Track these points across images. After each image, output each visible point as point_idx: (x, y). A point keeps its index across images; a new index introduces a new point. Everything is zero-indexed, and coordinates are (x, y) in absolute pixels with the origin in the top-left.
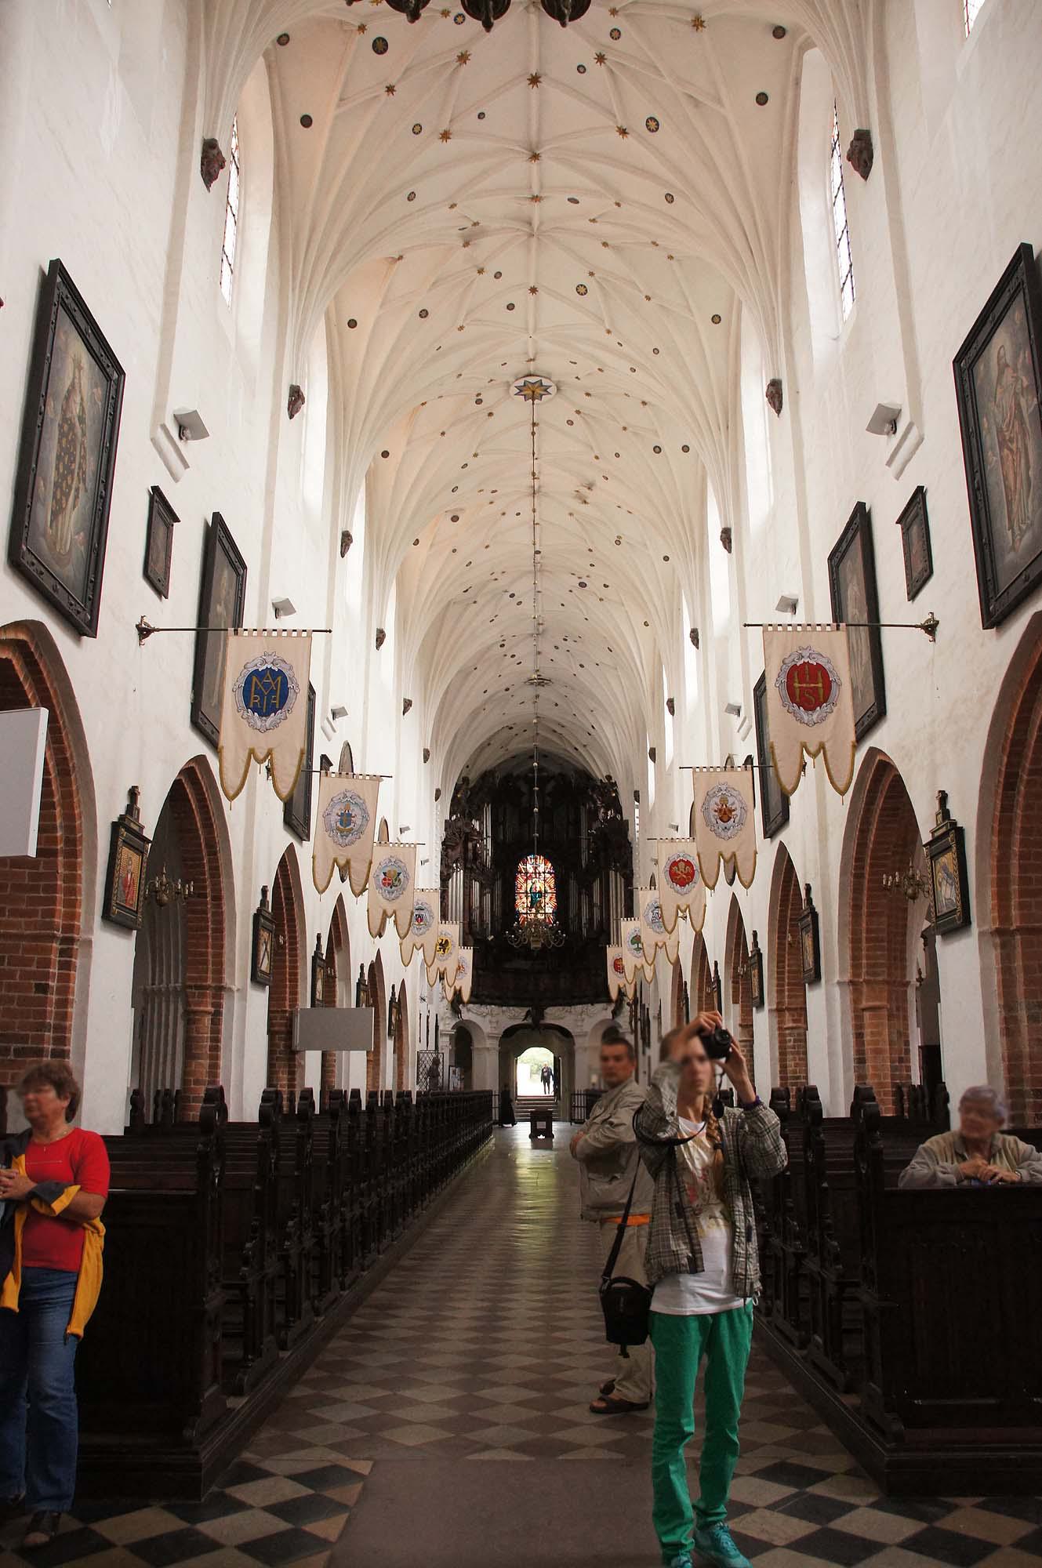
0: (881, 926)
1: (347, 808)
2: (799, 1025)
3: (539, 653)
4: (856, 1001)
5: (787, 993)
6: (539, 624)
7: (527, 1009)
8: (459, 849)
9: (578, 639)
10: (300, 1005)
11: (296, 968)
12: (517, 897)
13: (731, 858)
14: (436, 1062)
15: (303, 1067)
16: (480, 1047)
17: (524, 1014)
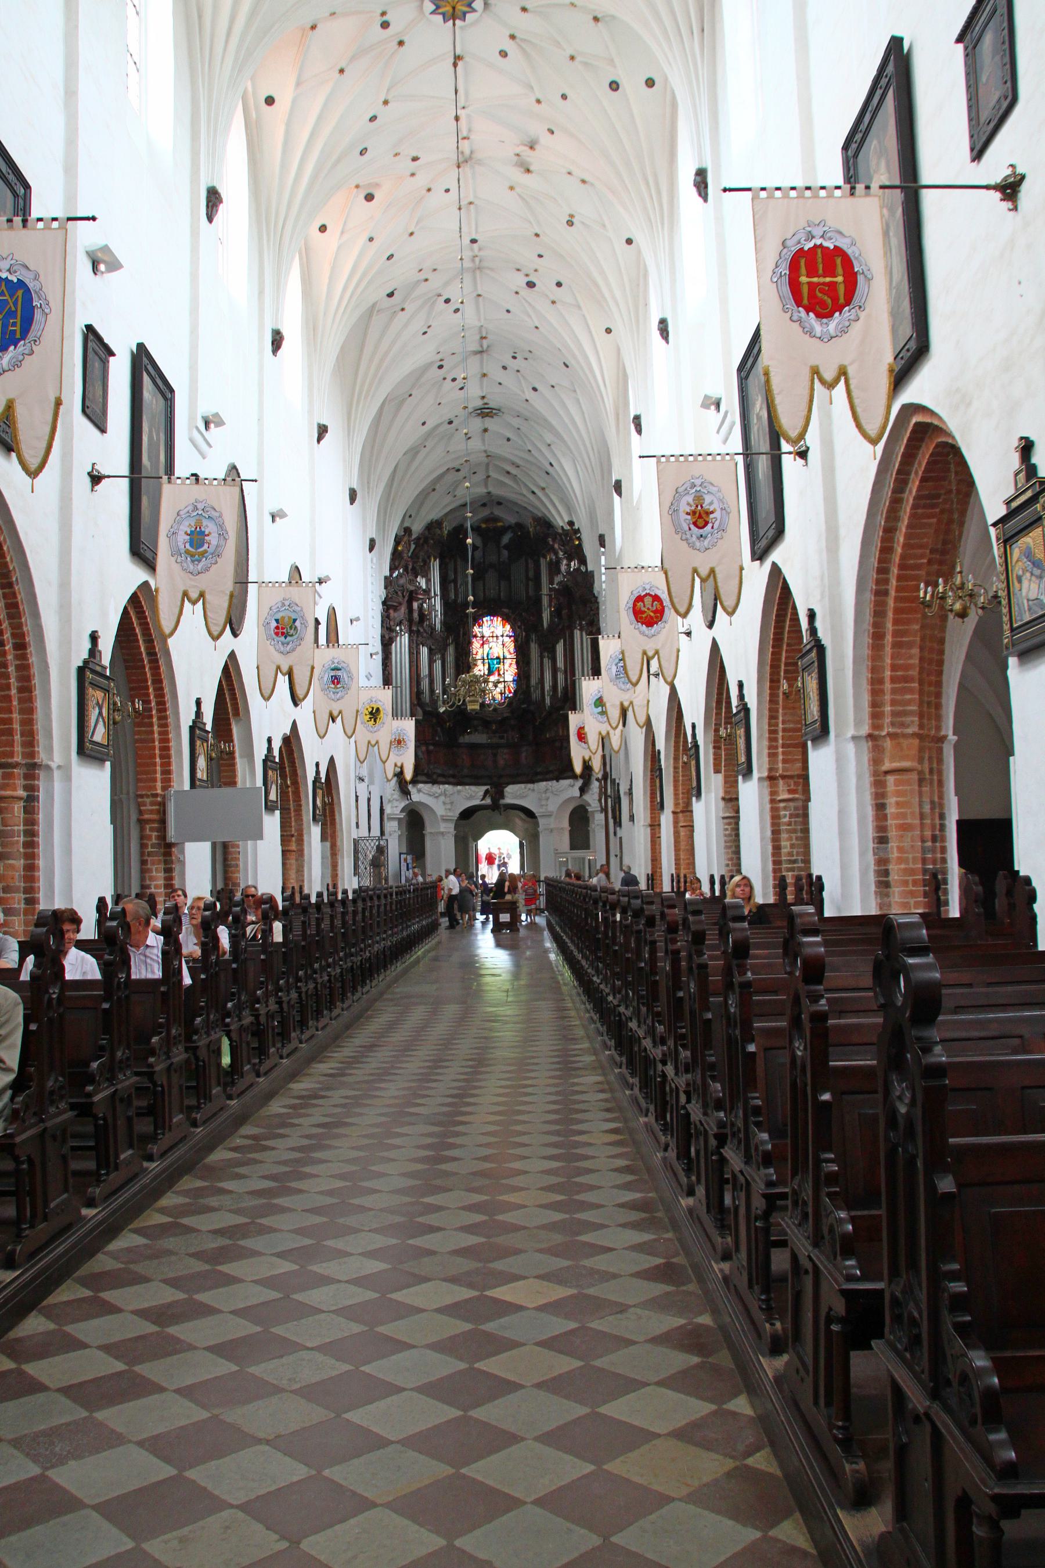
0: (912, 661)
1: (199, 524)
2: (797, 796)
3: (484, 375)
4: (876, 761)
5: (781, 757)
6: (482, 338)
7: (486, 788)
8: (403, 609)
9: (527, 355)
10: (175, 786)
11: (168, 740)
13: (709, 576)
14: (381, 850)
15: (182, 863)
16: (433, 831)
17: (482, 793)
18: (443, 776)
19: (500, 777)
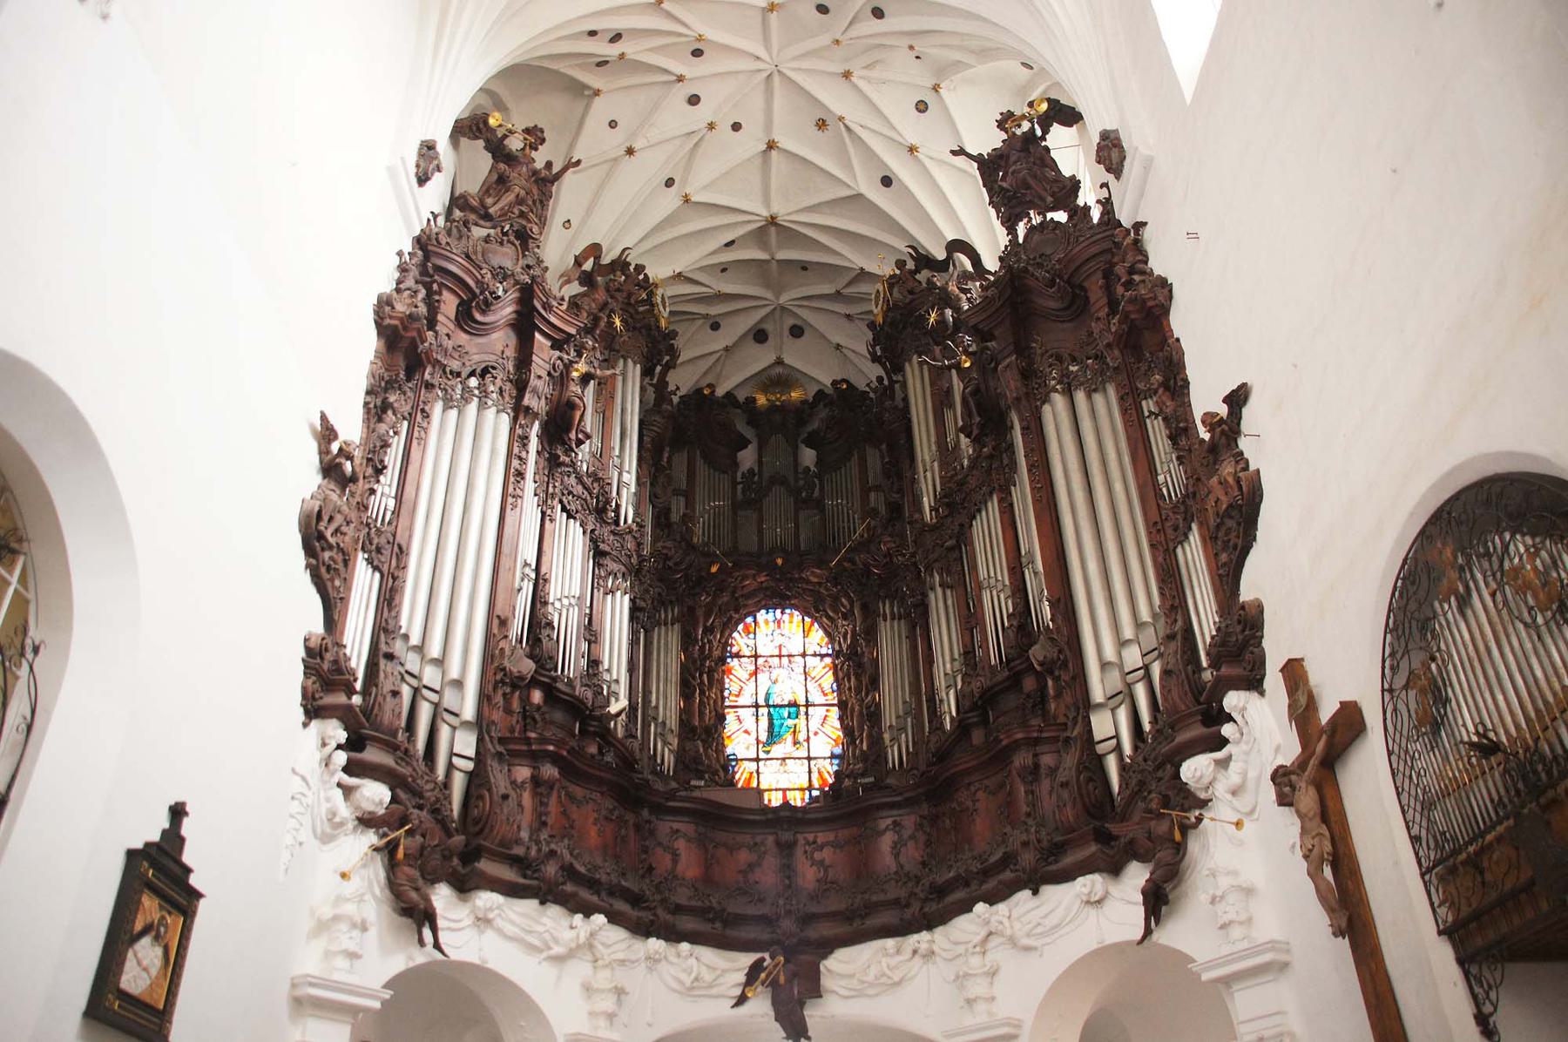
12: (730, 717)
17: (741, 977)
18: (592, 884)
19: (808, 919)
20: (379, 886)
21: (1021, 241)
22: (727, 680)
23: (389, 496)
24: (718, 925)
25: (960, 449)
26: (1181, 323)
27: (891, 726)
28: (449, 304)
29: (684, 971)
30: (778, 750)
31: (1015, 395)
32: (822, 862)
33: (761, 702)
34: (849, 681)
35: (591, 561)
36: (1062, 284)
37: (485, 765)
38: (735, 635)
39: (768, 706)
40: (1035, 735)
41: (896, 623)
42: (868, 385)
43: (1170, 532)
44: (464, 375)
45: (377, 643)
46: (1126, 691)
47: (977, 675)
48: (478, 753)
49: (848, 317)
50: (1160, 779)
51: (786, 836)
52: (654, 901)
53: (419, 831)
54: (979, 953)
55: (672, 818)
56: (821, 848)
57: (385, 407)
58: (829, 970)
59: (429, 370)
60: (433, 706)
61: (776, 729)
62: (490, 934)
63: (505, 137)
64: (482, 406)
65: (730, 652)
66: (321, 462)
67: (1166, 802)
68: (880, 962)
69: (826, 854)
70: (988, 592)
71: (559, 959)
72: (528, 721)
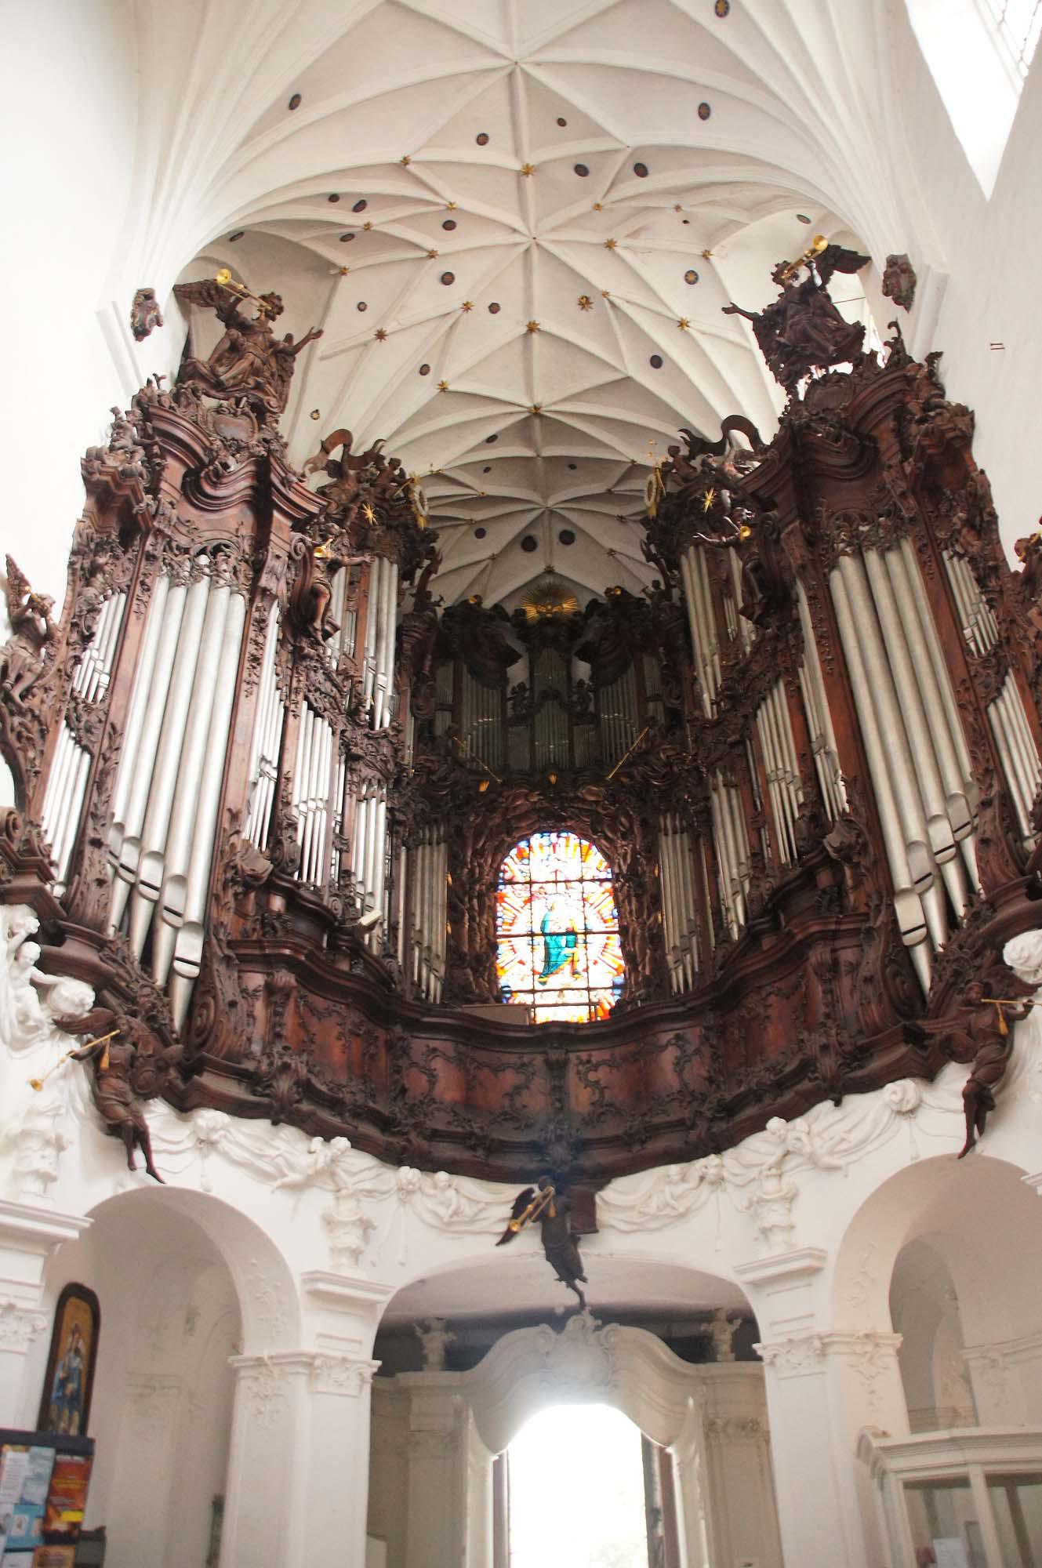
12: (504, 948)
17: (507, 1211)
18: (334, 1104)
19: (582, 1146)
20: (83, 1100)
21: (801, 397)
22: (499, 908)
23: (101, 673)
24: (480, 1153)
25: (742, 636)
26: (983, 454)
27: (675, 947)
28: (174, 472)
29: (442, 1204)
30: (554, 981)
31: (799, 562)
32: (597, 1082)
33: (537, 930)
34: (630, 904)
35: (343, 767)
36: (849, 436)
37: (211, 971)
38: (507, 860)
39: (544, 934)
40: (833, 927)
41: (678, 837)
42: (644, 591)
43: (981, 691)
44: (193, 552)
45: (84, 829)
46: (935, 872)
47: (768, 876)
48: (204, 957)
49: (621, 519)
50: (979, 968)
51: (556, 1055)
52: (407, 1125)
53: (130, 1039)
54: (775, 1176)
55: (428, 1036)
56: (595, 1068)
57: (95, 569)
58: (606, 1202)
59: (150, 540)
60: (152, 904)
61: (553, 959)
62: (214, 1159)
63: (238, 300)
64: (213, 586)
65: (503, 879)
66: (10, 614)
67: (987, 991)
68: (662, 1191)
69: (601, 1075)
70: (776, 785)
71: (295, 1188)
72: (267, 929)
